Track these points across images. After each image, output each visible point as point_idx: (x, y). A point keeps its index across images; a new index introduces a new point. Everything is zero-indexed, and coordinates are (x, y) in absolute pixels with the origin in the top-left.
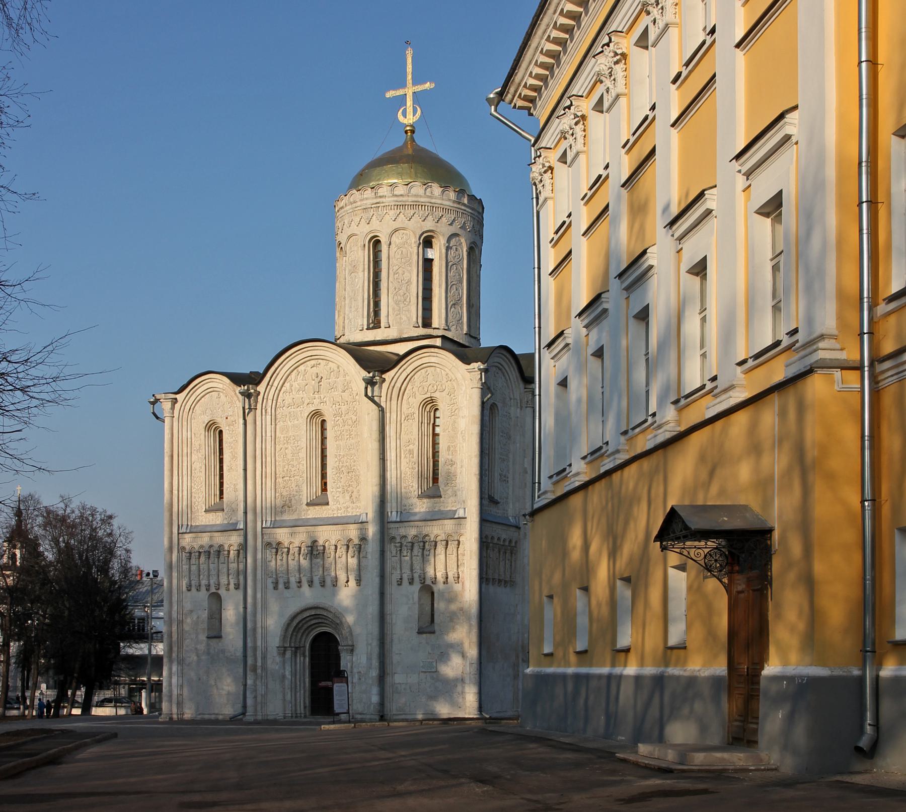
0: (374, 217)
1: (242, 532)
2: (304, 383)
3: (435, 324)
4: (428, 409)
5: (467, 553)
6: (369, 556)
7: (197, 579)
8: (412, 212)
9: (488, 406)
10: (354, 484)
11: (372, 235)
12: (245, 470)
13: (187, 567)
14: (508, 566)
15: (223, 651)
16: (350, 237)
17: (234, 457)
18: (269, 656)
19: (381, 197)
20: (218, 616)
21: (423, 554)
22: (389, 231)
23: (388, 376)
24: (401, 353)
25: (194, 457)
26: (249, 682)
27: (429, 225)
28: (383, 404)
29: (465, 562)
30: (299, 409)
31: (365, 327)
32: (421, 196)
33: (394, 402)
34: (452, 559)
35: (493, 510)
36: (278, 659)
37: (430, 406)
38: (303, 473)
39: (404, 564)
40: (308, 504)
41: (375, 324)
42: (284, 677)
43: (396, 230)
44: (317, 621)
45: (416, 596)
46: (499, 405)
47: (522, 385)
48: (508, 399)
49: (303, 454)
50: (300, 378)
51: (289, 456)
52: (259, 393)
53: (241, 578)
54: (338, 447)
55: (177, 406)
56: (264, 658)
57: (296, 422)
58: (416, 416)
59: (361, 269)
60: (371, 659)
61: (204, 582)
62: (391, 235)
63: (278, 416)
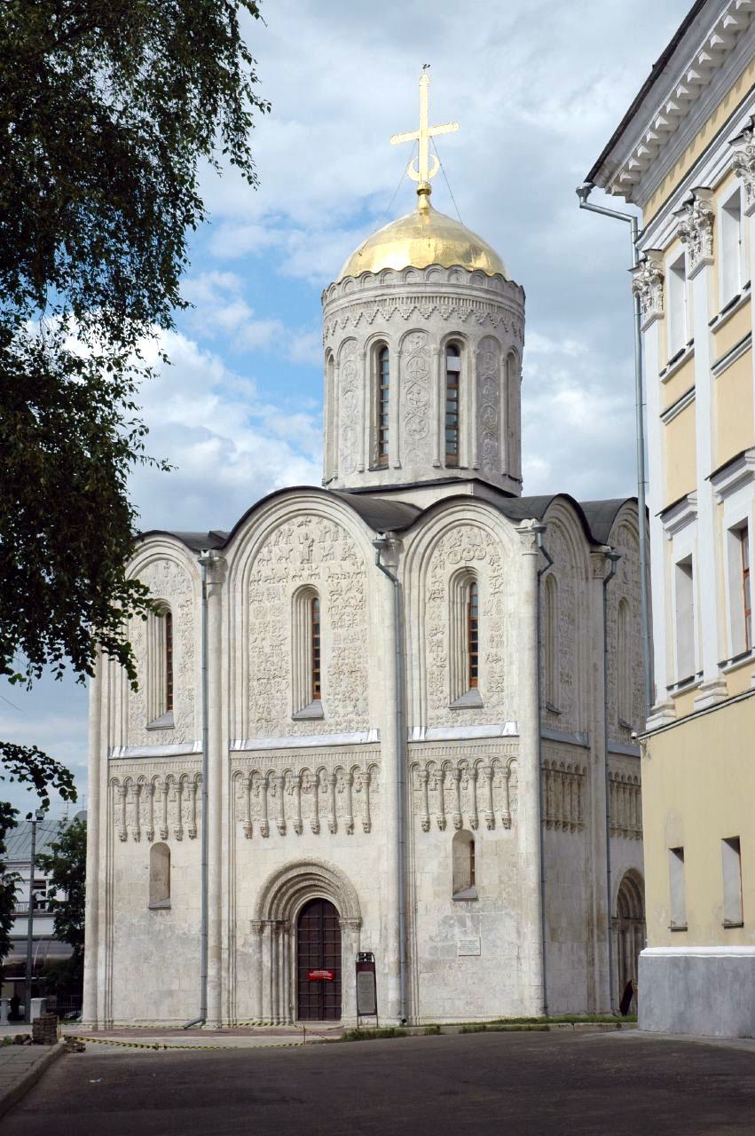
0: (379, 315)
1: (201, 757)
2: (289, 547)
3: (464, 462)
4: (461, 584)
5: (522, 785)
6: (381, 790)
7: (134, 824)
8: (431, 306)
9: (543, 578)
10: (360, 689)
11: (376, 339)
12: (205, 669)
13: (121, 806)
14: (575, 803)
15: (172, 928)
16: (344, 342)
17: (189, 653)
18: (238, 934)
20: (164, 878)
21: (458, 788)
23: (407, 540)
24: (425, 506)
26: (211, 972)
27: (454, 325)
28: (400, 577)
31: (367, 467)
32: (442, 285)
33: (415, 574)
34: (500, 793)
35: (553, 722)
36: (253, 939)
37: (467, 579)
39: (432, 801)
40: (295, 720)
41: (380, 463)
42: (260, 963)
44: (307, 883)
45: (450, 845)
46: (558, 576)
47: (587, 548)
48: (569, 567)
49: (287, 647)
50: (282, 541)
51: (267, 650)
53: (200, 822)
54: (337, 639)
56: (232, 937)
57: (277, 602)
58: (446, 593)
59: (361, 387)
60: (386, 938)
61: (145, 829)
62: (403, 339)
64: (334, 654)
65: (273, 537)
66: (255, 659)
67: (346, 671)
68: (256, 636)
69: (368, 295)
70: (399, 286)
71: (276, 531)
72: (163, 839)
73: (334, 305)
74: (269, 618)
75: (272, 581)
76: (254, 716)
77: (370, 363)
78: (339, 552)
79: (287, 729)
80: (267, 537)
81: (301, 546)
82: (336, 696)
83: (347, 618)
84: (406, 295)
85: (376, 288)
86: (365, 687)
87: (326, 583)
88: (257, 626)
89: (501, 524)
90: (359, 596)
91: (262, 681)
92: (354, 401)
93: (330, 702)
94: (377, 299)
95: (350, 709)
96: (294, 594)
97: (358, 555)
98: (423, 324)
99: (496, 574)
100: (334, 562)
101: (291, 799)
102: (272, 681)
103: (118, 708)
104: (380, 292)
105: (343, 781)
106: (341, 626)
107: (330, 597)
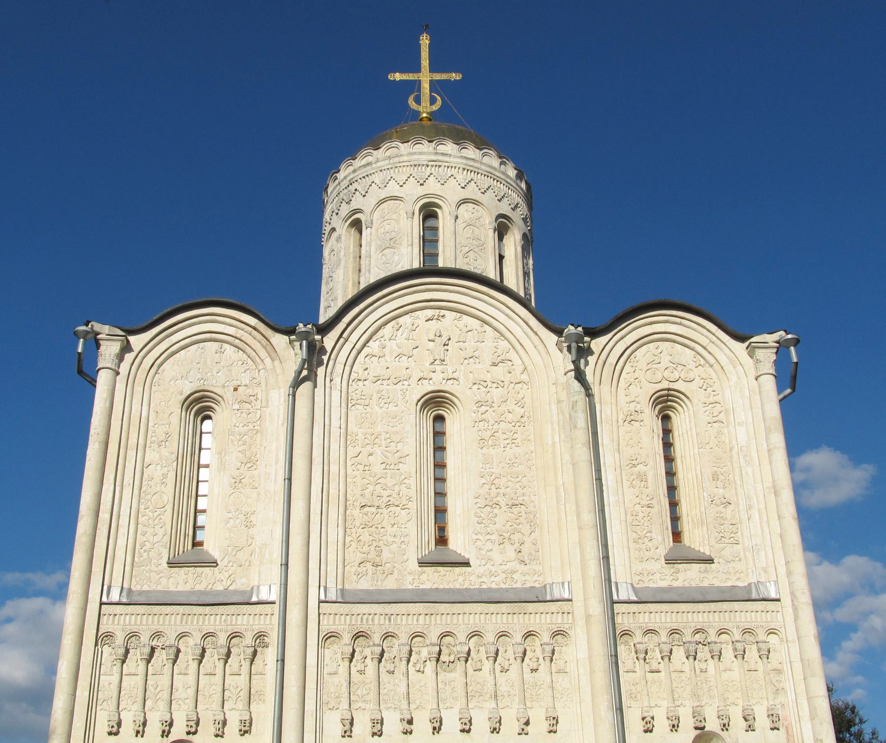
1: (276, 608)
10: (526, 529)
19: (443, 154)
22: (457, 199)
25: (151, 455)
29: (788, 686)
33: (605, 387)
37: (665, 404)
38: (410, 500)
40: (422, 563)
43: (465, 201)
49: (409, 466)
50: (401, 336)
51: (378, 469)
52: (323, 350)
55: (129, 357)
62: (459, 205)
63: (353, 395)
64: (483, 481)
65: (387, 330)
66: (358, 479)
67: (502, 504)
69: (424, 159)
70: (455, 157)
71: (393, 323)
72: (188, 733)
73: (368, 168)
76: (354, 556)
77: (415, 225)
78: (487, 358)
79: (410, 578)
82: (489, 537)
84: (463, 166)
85: (430, 153)
87: (469, 392)
88: (360, 437)
89: (718, 342)
90: (519, 411)
91: (366, 509)
92: (396, 258)
93: (479, 543)
94: (430, 163)
95: (511, 553)
96: (419, 401)
98: (478, 196)
99: (712, 400)
100: (480, 366)
101: (425, 679)
102: (385, 511)
103: (123, 531)
104: (434, 158)
105: (509, 653)
106: (493, 446)
107: (475, 408)
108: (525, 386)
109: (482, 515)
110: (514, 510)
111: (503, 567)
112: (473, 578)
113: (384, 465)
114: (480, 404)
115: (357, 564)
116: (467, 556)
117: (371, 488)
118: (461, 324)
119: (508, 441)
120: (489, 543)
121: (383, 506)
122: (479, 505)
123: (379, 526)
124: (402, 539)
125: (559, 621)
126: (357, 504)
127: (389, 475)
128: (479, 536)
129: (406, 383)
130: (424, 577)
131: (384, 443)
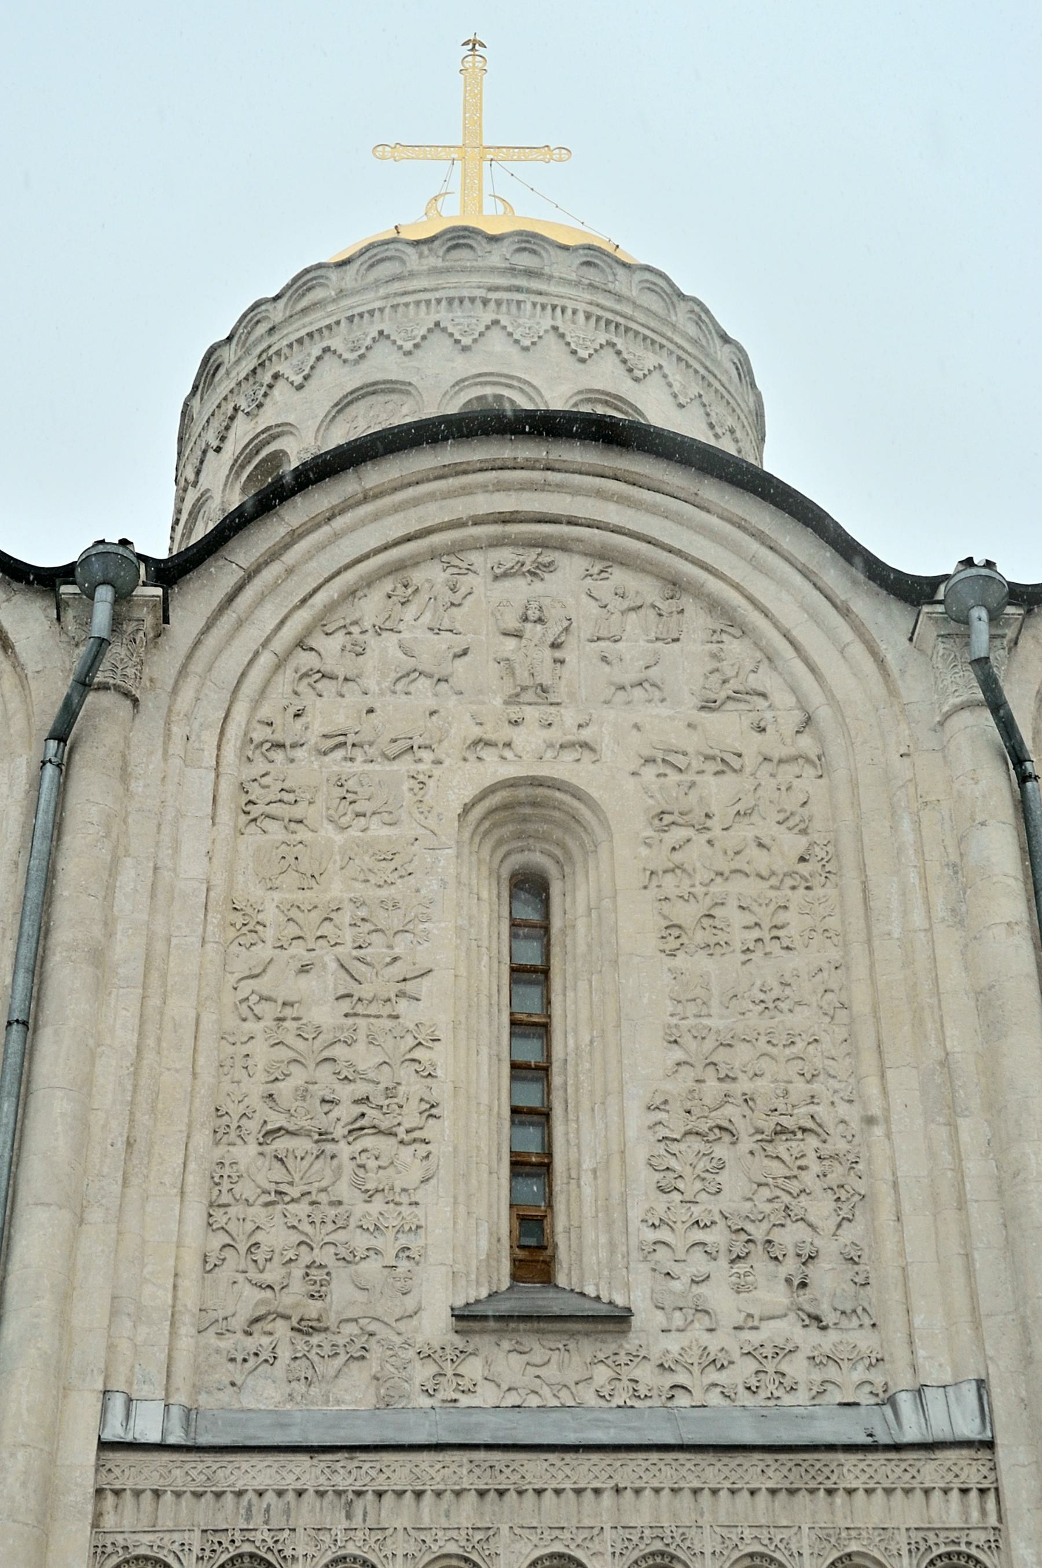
10: (821, 1209)
30: (405, 765)
51: (325, 1014)
57: (377, 830)
64: (678, 1054)
65: (371, 607)
67: (742, 1127)
68: (263, 952)
71: (388, 585)
74: (336, 889)
75: (358, 753)
80: (351, 594)
81: (511, 643)
82: (698, 1235)
83: (741, 919)
86: (849, 1203)
87: (630, 785)
91: (281, 1144)
96: (467, 809)
97: (782, 698)
100: (664, 711)
102: (344, 1151)
107: (649, 832)
108: (809, 772)
109: (673, 1163)
110: (781, 1148)
111: (746, 1335)
112: (646, 1374)
113: (346, 1006)
114: (668, 819)
115: (239, 1323)
116: (620, 1301)
117: (298, 1076)
118: (604, 589)
119: (756, 933)
120: (698, 1254)
121: (339, 1132)
122: (662, 1132)
123: (323, 1198)
124: (403, 1240)
125: (954, 1519)
126: (252, 1126)
127: (361, 1035)
128: (664, 1234)
129: (425, 755)
130: (473, 1368)
131: (348, 935)
